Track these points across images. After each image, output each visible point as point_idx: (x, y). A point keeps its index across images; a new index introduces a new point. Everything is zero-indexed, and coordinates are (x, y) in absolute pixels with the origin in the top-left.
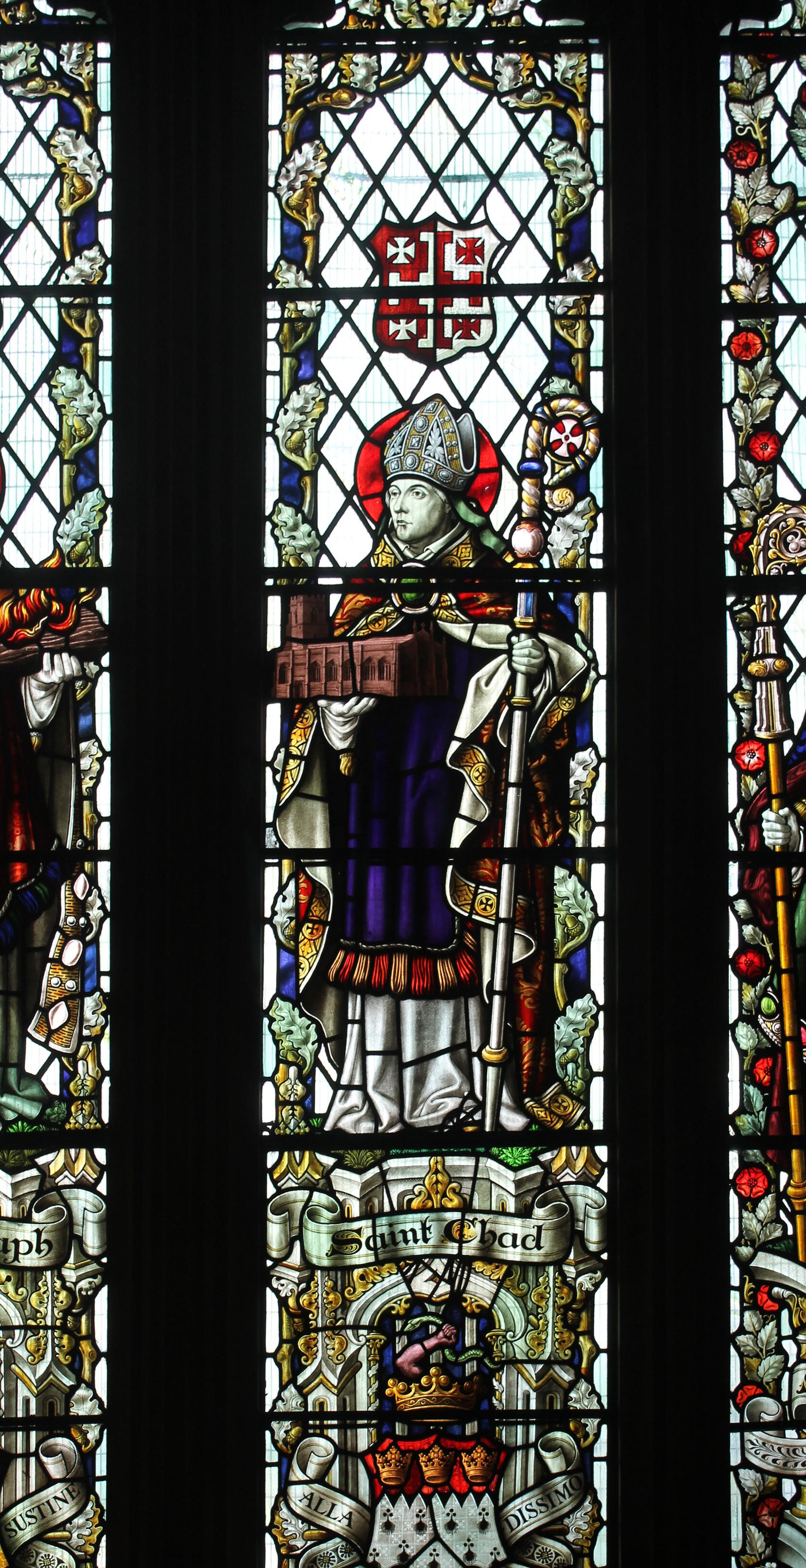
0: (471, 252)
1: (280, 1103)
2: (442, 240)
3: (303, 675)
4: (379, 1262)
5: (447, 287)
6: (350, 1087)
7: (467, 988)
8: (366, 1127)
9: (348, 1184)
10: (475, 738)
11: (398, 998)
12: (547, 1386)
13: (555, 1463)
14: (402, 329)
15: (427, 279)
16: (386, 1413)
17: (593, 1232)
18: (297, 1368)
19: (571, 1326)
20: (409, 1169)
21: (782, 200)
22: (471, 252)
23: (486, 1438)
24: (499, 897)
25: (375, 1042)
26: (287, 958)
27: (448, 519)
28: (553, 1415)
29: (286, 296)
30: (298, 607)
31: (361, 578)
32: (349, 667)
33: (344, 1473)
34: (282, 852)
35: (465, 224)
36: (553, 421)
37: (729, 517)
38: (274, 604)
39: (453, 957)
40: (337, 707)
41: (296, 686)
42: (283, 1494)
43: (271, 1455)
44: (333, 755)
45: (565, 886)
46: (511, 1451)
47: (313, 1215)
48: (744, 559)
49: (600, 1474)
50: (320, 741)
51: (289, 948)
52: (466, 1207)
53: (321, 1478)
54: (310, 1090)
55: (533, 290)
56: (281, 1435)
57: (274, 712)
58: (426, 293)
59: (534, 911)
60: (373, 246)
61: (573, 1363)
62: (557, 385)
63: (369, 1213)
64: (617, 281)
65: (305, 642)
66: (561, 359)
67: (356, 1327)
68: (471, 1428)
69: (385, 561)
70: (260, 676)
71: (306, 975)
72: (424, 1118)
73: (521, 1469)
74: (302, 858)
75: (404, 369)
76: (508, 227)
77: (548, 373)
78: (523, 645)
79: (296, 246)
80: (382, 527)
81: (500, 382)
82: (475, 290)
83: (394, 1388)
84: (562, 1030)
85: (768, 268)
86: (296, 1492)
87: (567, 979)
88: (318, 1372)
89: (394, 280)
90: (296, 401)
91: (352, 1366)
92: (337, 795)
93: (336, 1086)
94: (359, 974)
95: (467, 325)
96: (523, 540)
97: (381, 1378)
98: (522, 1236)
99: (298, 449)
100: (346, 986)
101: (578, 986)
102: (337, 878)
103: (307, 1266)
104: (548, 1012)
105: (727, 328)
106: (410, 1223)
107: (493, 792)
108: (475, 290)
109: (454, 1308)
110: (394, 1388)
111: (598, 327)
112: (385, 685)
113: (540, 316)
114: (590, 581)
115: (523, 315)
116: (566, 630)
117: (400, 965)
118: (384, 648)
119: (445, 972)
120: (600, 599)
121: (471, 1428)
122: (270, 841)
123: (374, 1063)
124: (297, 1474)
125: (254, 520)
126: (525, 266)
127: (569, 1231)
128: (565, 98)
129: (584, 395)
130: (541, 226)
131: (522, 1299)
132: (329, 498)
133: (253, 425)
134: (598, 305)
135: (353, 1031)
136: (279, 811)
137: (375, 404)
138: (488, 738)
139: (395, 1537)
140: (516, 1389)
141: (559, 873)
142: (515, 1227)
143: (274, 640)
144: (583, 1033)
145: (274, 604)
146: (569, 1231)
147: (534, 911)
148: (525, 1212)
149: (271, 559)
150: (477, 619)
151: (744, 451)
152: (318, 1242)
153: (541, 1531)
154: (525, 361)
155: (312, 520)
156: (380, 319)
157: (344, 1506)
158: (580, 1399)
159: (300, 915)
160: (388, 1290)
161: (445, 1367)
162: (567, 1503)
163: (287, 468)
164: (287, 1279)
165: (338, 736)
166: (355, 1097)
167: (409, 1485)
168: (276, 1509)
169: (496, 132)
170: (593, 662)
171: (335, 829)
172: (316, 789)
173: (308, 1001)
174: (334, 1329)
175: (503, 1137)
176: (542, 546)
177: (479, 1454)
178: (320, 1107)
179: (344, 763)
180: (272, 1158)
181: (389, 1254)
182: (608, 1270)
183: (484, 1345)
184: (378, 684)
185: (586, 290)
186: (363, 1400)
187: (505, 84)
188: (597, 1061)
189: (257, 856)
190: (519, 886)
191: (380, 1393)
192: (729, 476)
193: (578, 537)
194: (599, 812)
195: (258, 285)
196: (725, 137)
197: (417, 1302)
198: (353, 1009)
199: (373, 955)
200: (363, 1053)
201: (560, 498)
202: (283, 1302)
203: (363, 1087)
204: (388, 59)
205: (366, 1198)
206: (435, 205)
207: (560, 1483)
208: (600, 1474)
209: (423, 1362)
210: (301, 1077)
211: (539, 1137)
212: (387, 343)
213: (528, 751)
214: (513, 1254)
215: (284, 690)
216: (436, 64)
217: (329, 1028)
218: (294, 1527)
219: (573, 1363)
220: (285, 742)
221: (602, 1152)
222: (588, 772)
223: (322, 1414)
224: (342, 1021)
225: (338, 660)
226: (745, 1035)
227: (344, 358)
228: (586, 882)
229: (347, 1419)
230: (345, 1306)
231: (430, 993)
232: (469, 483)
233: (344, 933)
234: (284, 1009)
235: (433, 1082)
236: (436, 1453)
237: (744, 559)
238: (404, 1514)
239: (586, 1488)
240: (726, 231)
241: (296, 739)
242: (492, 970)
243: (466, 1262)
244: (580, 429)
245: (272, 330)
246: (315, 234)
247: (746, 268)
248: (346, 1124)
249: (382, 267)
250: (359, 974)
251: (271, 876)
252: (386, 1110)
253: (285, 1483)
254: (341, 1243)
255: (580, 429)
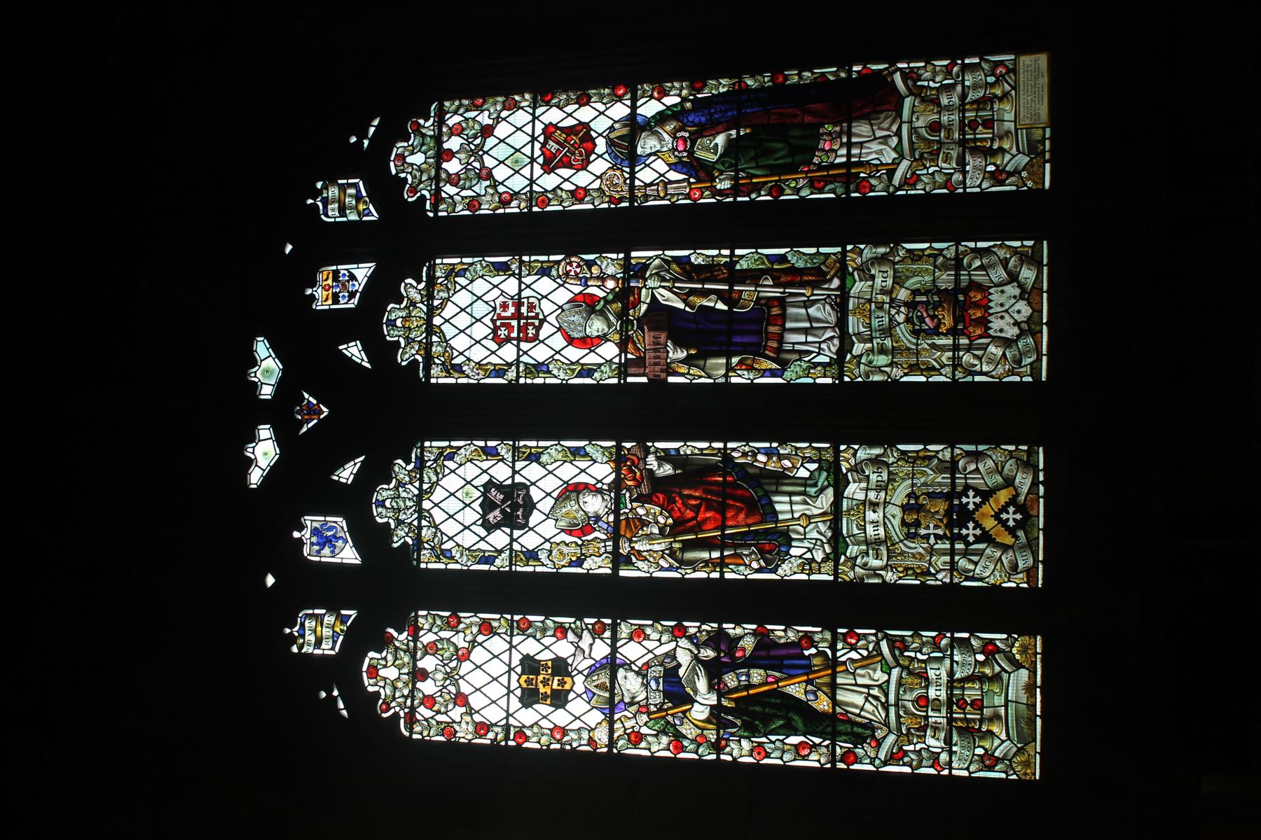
0: (504, 306)
1: (825, 376)
2: (500, 317)
3: (658, 368)
4: (891, 336)
5: (518, 316)
6: (820, 348)
7: (782, 302)
8: (836, 342)
9: (858, 348)
10: (684, 301)
11: (785, 330)
12: (944, 267)
13: (977, 263)
14: (531, 332)
15: (514, 323)
16: (953, 332)
17: (882, 250)
18: (933, 368)
19: (920, 258)
20: (854, 325)
21: (491, 191)
22: (504, 306)
23: (965, 291)
24: (747, 291)
25: (802, 338)
26: (767, 373)
27: (602, 313)
28: (957, 264)
29: (518, 377)
30: (631, 370)
31: (622, 346)
32: (655, 350)
33: (978, 349)
34: (726, 376)
35: (495, 309)
36: (567, 274)
37: (605, 206)
38: (630, 380)
39: (769, 308)
40: (671, 355)
41: (662, 371)
42: (986, 374)
43: (969, 379)
44: (689, 357)
45: (743, 265)
46: (971, 282)
47: (871, 362)
48: (621, 200)
49: (981, 245)
50: (683, 361)
51: (764, 373)
52: (870, 301)
53: (980, 358)
54: (820, 364)
55: (520, 282)
56: (961, 375)
57: (671, 379)
58: (519, 322)
59: (753, 276)
60: (501, 343)
61: (935, 257)
62: (554, 272)
63: (871, 341)
64: (517, 249)
65: (645, 368)
66: (544, 272)
67: (917, 345)
68: (961, 298)
69: (617, 337)
70: (657, 384)
71: (774, 366)
72: (833, 319)
73: (979, 277)
74: (729, 368)
75: (546, 330)
76: (496, 292)
77: (549, 276)
78: (650, 283)
79: (500, 372)
80: (604, 338)
81: (552, 294)
82: (518, 305)
83: (943, 329)
84: (801, 264)
85: (515, 195)
86: (985, 368)
87: (780, 263)
88: (935, 360)
89: (514, 335)
90: (555, 372)
91: (933, 346)
92: (704, 355)
93: (819, 354)
94: (774, 345)
95: (531, 307)
96: (610, 284)
97: (938, 334)
98: (883, 279)
99: (573, 370)
100: (779, 350)
101: (783, 259)
102: (736, 355)
103: (891, 365)
104: (793, 270)
105: (535, 209)
106: (875, 323)
107: (705, 293)
108: (518, 305)
109: (911, 305)
110: (943, 329)
111: (533, 258)
112: (663, 336)
113: (528, 280)
114: (628, 258)
115: (528, 286)
116: (645, 267)
117: (772, 329)
118: (649, 336)
119: (775, 311)
120: (634, 254)
121: (961, 298)
122: (722, 380)
123: (810, 339)
124: (978, 368)
125: (598, 387)
126: (511, 286)
127: (881, 260)
128: (452, 273)
129: (558, 263)
130: (496, 280)
131: (908, 278)
132: (592, 359)
133: (564, 388)
134: (526, 258)
135: (797, 347)
136: (709, 377)
137: (558, 341)
138: (685, 296)
139: (1006, 328)
140: (946, 280)
141: (738, 267)
142: (878, 281)
143: (644, 380)
144: (802, 256)
145: (630, 380)
146: (881, 260)
147: (753, 276)
148: (873, 278)
149: (615, 381)
150: (639, 301)
151: (581, 201)
152: (882, 360)
153: (1005, 268)
154: (545, 285)
155: (600, 365)
156: (528, 340)
157: (992, 349)
158: (951, 253)
159: (750, 368)
160: (903, 332)
161: (935, 309)
162: (994, 258)
163: (580, 375)
164: (896, 373)
165: (682, 354)
166: (824, 346)
167: (984, 322)
168: (992, 377)
169: (462, 298)
170: (657, 256)
171: (717, 355)
172: (701, 363)
173: (784, 365)
174: (918, 353)
175: (842, 287)
176: (613, 277)
177: (972, 294)
178: (827, 360)
179: (693, 352)
180: (847, 379)
181: (888, 331)
182: (897, 244)
183: (926, 293)
184: (662, 340)
185: (522, 262)
186: (948, 341)
187: (445, 295)
188: (813, 250)
189: (728, 384)
190: (743, 283)
191: (945, 335)
192: (590, 206)
193: (610, 263)
194: (715, 252)
195: (513, 387)
196: (467, 213)
197: (908, 320)
198: (789, 347)
199: (768, 339)
200: (806, 343)
201: (595, 270)
202: (906, 374)
203: (820, 343)
204: (435, 338)
205: (865, 341)
206: (487, 320)
207: (985, 261)
208: (981, 245)
209: (933, 317)
210: (814, 368)
211: (843, 273)
212: (536, 337)
213: (691, 280)
214: (890, 282)
215: (663, 375)
216: (437, 321)
217: (796, 356)
218: (1000, 370)
219: (935, 257)
220: (682, 375)
221: (849, 247)
222: (698, 258)
223: (953, 358)
224: (793, 351)
225: (653, 354)
226: (804, 193)
227: (540, 353)
228: (742, 257)
229: (956, 348)
230: (908, 349)
231: (783, 317)
232: (587, 305)
233: (757, 350)
234: (788, 375)
235: (819, 315)
236: (971, 312)
237: (621, 200)
238: (996, 324)
239: (987, 251)
240: (501, 211)
241: (682, 371)
242: (775, 292)
243: (892, 300)
244: (570, 264)
245: (529, 381)
246: (495, 365)
247: (514, 203)
248: (834, 349)
249: (508, 339)
250: (774, 345)
251: (734, 380)
252: (829, 334)
253: (981, 373)
254: (882, 351)
255: (570, 264)
